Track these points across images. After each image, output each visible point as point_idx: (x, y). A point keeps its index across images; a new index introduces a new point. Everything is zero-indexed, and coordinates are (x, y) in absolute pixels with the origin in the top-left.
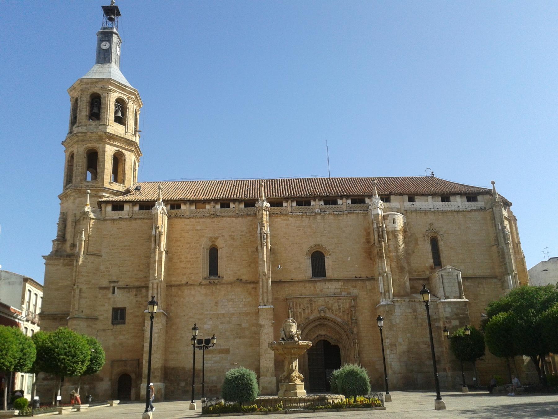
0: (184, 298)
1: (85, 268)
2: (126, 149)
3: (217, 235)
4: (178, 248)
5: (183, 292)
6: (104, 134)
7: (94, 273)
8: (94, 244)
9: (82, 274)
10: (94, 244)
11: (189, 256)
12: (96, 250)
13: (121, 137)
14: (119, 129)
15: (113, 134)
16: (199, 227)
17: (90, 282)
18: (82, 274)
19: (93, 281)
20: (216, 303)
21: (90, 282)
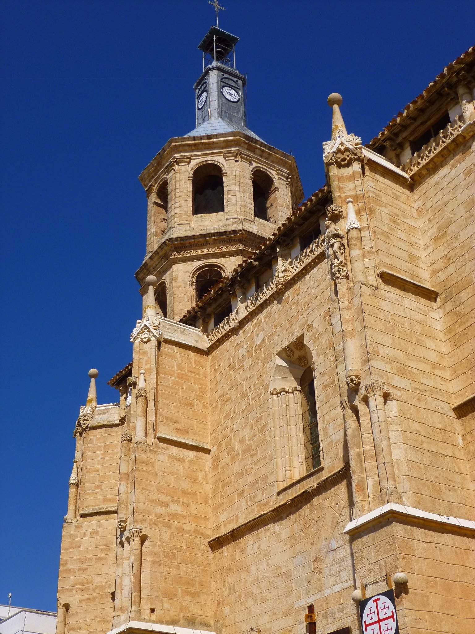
0: (247, 569)
1: (75, 550)
2: (223, 255)
3: (297, 334)
4: (228, 422)
5: (244, 551)
6: (166, 248)
7: (99, 559)
8: (98, 487)
9: (69, 566)
10: (98, 487)
11: (247, 432)
12: (104, 500)
13: (204, 236)
14: (206, 223)
15: (182, 239)
16: (259, 340)
17: (89, 583)
18: (69, 566)
19: (98, 580)
20: (316, 560)
21: (89, 583)
